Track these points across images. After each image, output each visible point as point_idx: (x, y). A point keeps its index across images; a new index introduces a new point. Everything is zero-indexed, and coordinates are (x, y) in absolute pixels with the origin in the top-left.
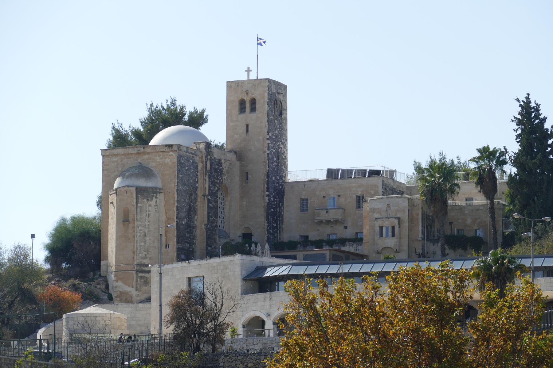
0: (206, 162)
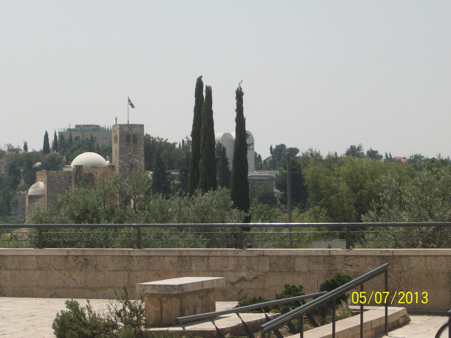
0: (76, 176)
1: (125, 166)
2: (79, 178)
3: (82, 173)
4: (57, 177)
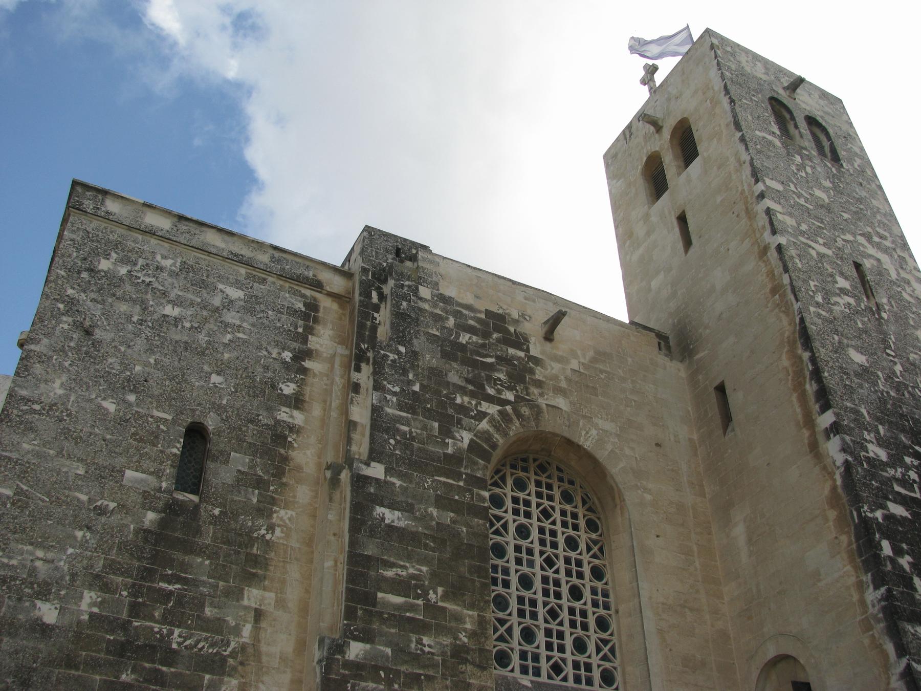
0: (368, 309)
1: (822, 256)
2: (399, 316)
3: (424, 292)
4: (167, 263)
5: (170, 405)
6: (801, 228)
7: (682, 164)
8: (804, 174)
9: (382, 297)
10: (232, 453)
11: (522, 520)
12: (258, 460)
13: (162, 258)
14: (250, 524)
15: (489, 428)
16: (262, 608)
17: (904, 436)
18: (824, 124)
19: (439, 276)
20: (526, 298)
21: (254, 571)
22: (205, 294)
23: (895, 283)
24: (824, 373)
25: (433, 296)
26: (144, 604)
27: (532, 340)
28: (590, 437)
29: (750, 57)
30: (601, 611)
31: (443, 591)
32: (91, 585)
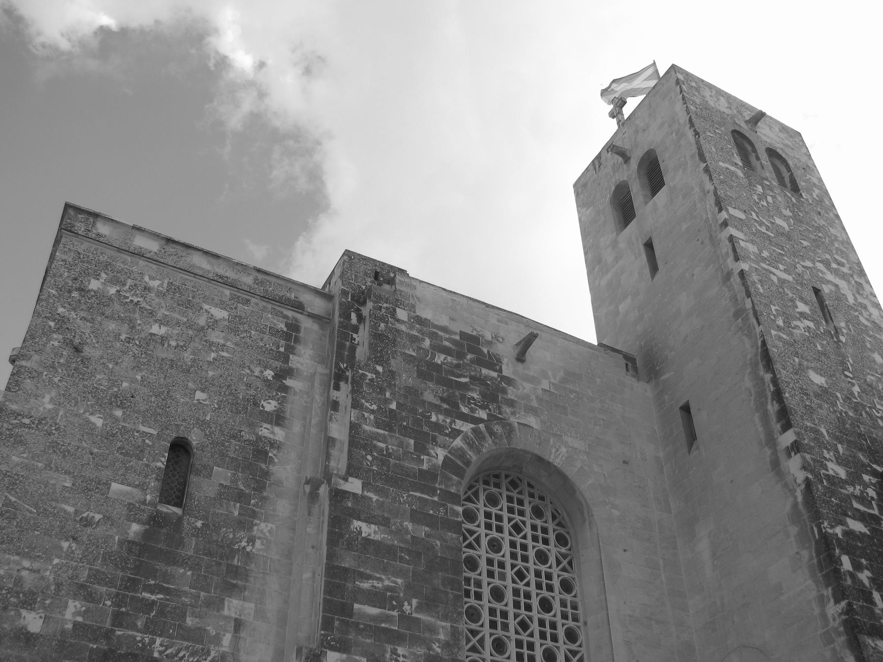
0: (347, 330)
1: (782, 282)
2: (377, 337)
3: (402, 314)
4: (155, 284)
5: (155, 421)
6: (762, 255)
7: (649, 193)
8: (765, 204)
9: (361, 319)
10: (215, 467)
11: (494, 534)
12: (240, 474)
13: (150, 279)
14: (231, 536)
15: (463, 445)
16: (242, 617)
17: (862, 455)
18: (784, 156)
19: (416, 299)
20: (499, 321)
21: (235, 582)
22: (191, 314)
23: (852, 308)
24: (785, 393)
25: (409, 318)
26: (127, 614)
27: (505, 361)
28: (560, 454)
29: (714, 92)
30: (570, 623)
31: (418, 602)
32: (75, 595)
